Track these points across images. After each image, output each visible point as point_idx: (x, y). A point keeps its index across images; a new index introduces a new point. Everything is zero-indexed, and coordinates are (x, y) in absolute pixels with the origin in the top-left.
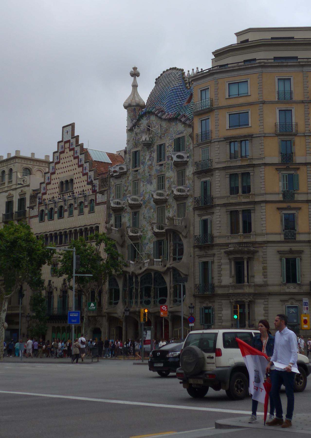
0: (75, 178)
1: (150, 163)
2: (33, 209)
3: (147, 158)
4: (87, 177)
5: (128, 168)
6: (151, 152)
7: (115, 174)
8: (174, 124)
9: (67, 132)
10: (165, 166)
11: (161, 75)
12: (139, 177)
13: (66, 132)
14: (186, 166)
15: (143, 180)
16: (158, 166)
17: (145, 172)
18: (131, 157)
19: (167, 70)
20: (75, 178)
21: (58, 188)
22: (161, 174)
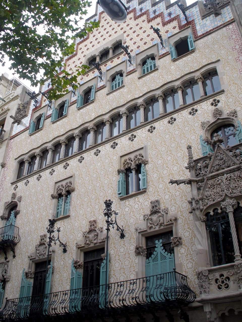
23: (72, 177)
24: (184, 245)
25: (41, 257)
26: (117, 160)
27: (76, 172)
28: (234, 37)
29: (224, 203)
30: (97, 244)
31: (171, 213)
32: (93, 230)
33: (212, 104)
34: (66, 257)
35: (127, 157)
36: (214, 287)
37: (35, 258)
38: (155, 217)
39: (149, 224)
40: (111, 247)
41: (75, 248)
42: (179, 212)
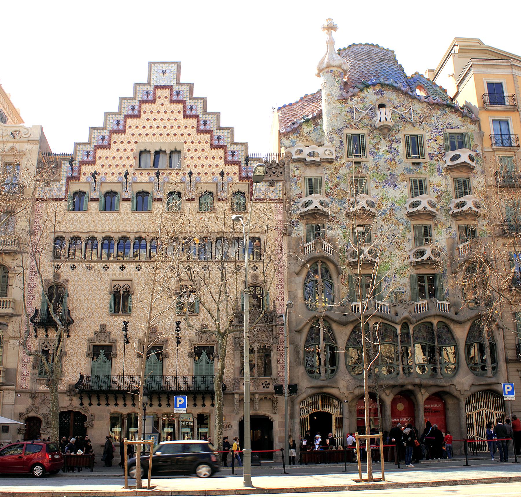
0: (189, 150)
1: (390, 156)
2: (47, 185)
3: (384, 146)
4: (226, 152)
5: (339, 155)
6: (392, 141)
7: (308, 159)
8: (439, 112)
9: (164, 73)
10: (425, 167)
11: (350, 47)
12: (364, 172)
13: (161, 71)
14: (471, 174)
15: (376, 179)
16: (411, 163)
17: (380, 168)
18: (345, 142)
19: (360, 44)
20: (189, 150)
21: (135, 158)
22: (418, 176)
28: (279, 217)
29: (254, 344)
33: (252, 268)
38: (204, 336)
39: (199, 340)
41: (137, 342)
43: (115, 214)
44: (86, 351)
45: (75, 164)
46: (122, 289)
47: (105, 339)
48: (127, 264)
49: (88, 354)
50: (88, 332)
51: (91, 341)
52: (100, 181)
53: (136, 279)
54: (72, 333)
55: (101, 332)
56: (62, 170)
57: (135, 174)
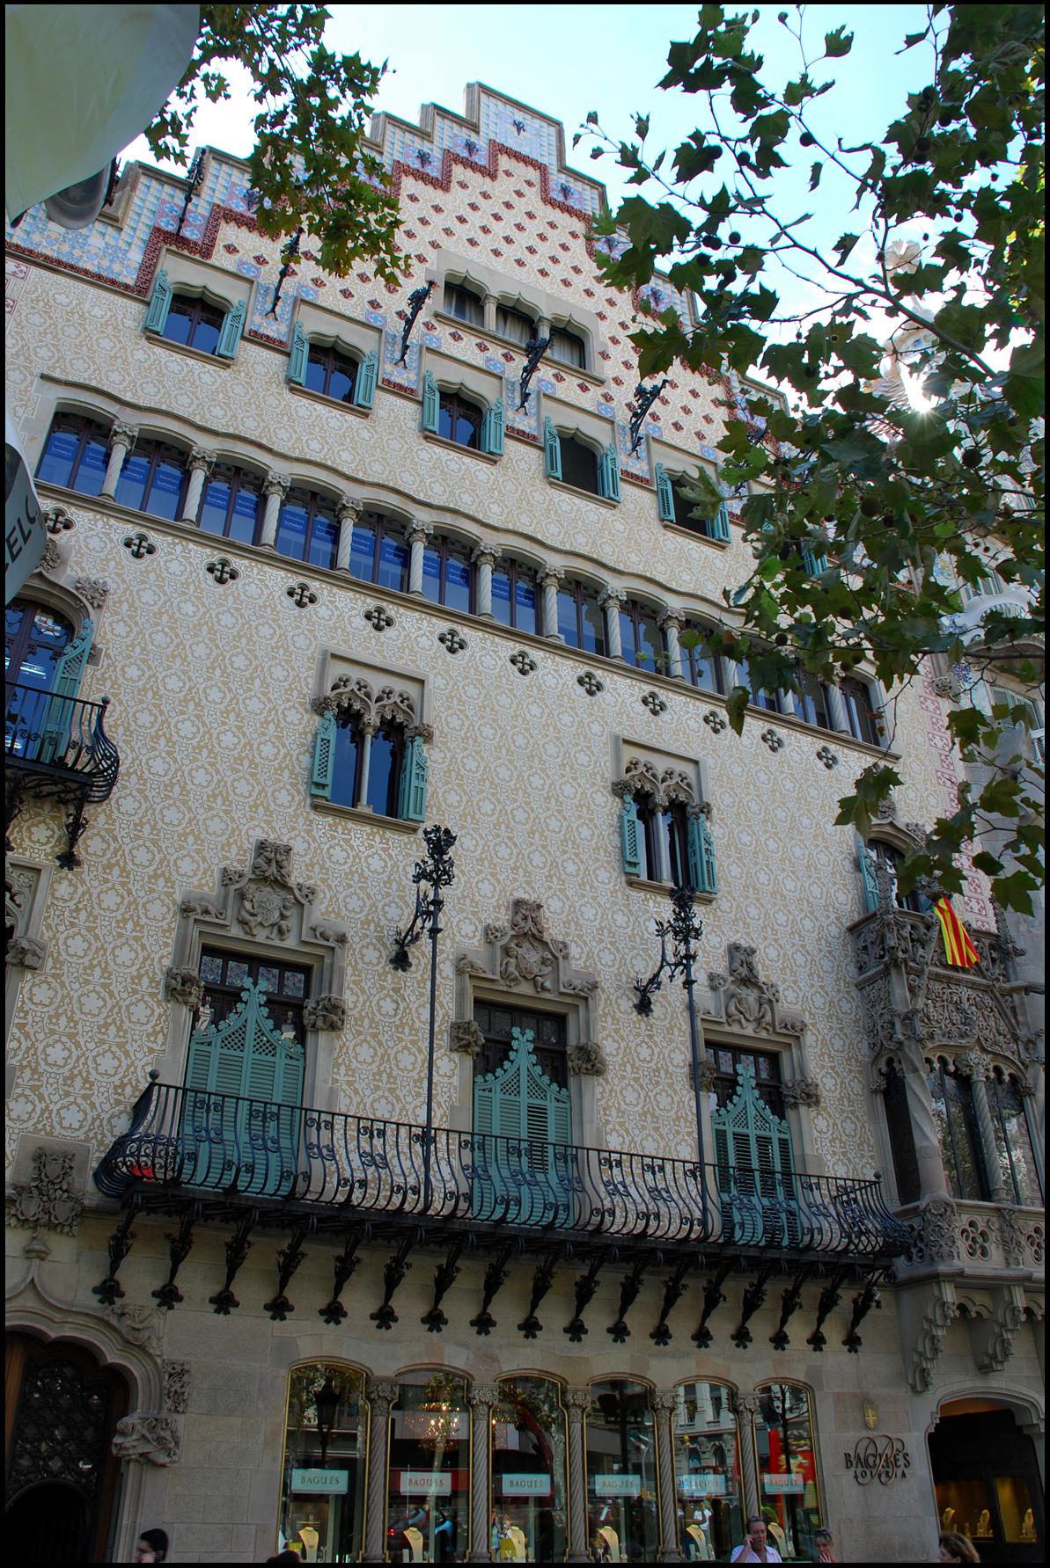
23: (422, 682)
24: (825, 1109)
25: (261, 936)
26: (603, 738)
27: (431, 676)
30: (546, 995)
31: (786, 1005)
32: (533, 935)
34: (408, 991)
35: (643, 756)
36: (962, 1245)
37: (223, 926)
38: (751, 996)
39: (732, 1009)
40: (604, 1028)
42: (807, 1014)
43: (350, 418)
44: (167, 962)
45: (196, 206)
46: (374, 707)
47: (283, 917)
48: (402, 610)
49: (186, 980)
50: (186, 866)
51: (206, 912)
52: (292, 292)
53: (440, 682)
54: (90, 846)
55: (262, 879)
56: (136, 200)
57: (433, 328)
